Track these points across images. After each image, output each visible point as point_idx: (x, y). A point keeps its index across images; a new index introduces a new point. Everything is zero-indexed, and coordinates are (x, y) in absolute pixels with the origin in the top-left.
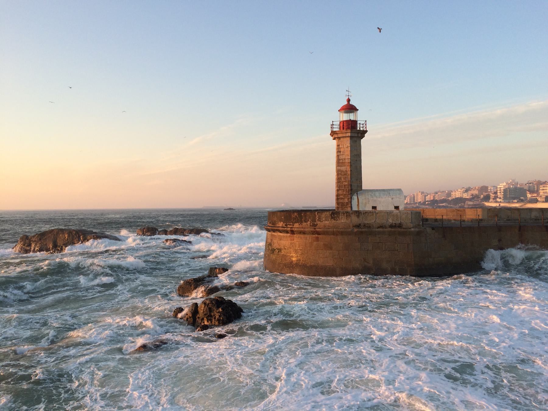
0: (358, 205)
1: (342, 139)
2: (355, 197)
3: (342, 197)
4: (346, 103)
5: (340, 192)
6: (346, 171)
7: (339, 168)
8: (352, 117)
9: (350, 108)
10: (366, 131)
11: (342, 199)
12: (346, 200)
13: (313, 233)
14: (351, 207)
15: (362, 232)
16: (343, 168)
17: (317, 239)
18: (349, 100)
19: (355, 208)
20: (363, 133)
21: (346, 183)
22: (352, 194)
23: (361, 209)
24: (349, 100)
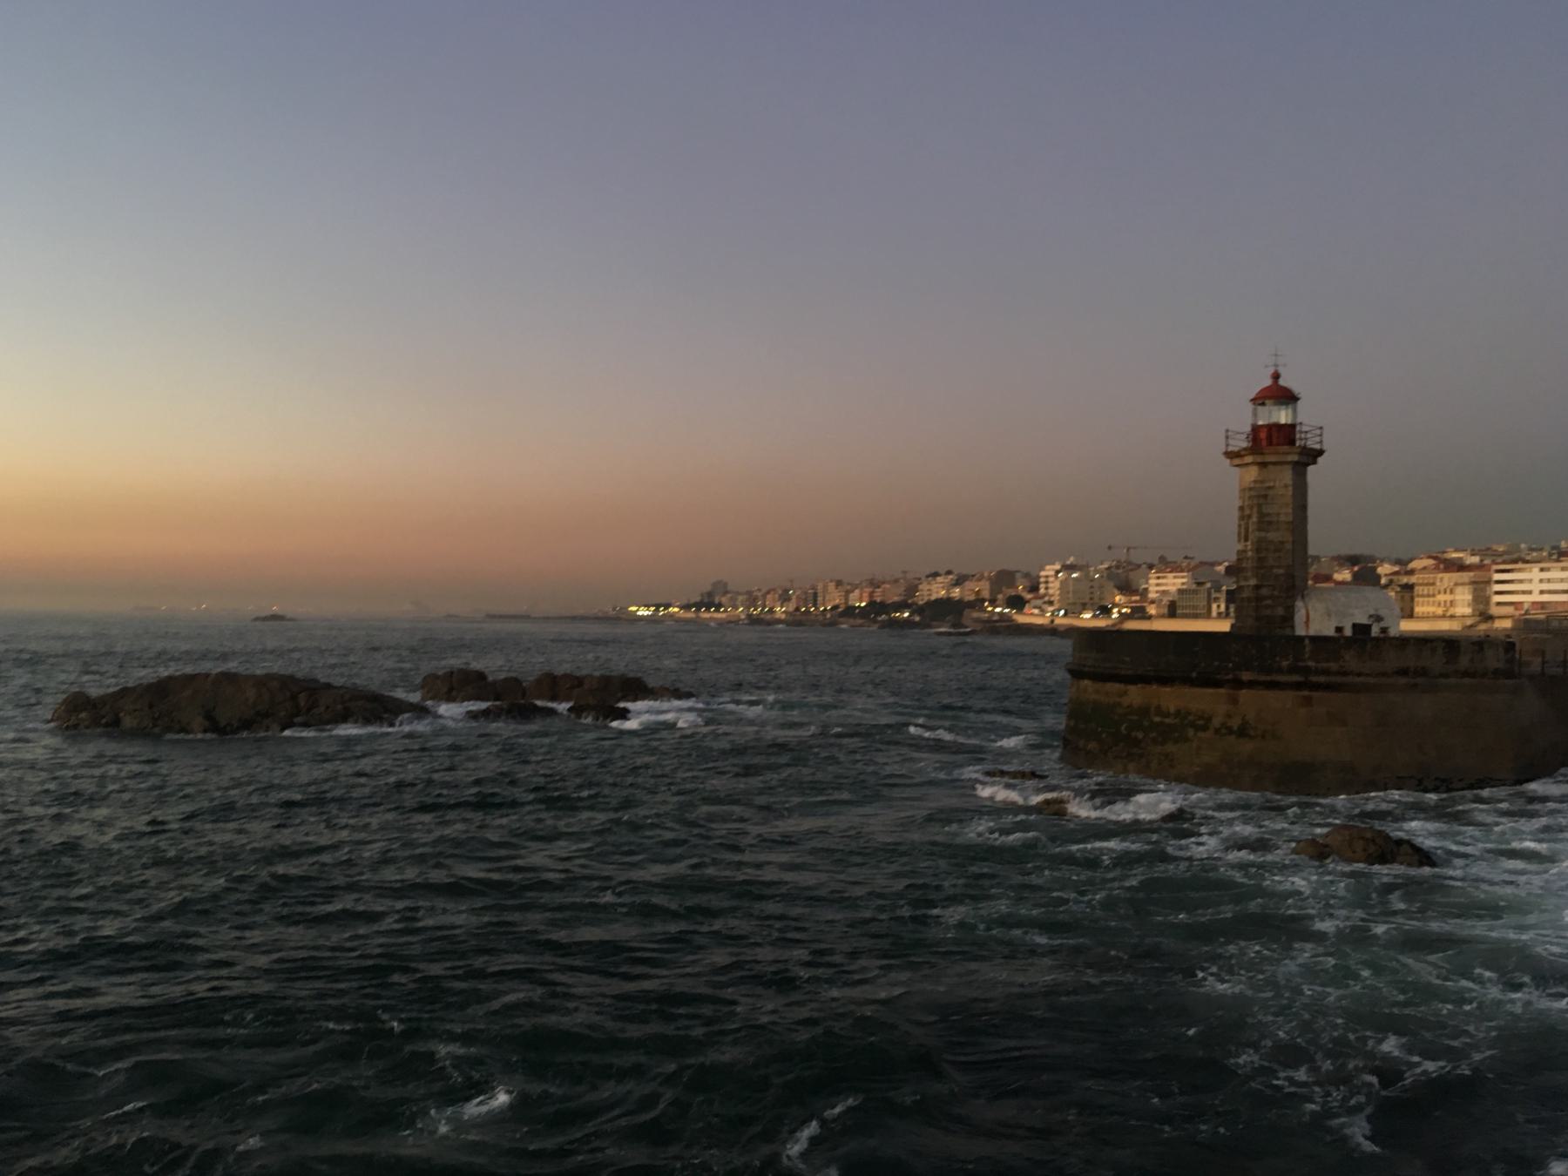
0: (1307, 622)
1: (1271, 467)
2: (1299, 604)
3: (1269, 602)
4: (1268, 382)
5: (1264, 592)
6: (1282, 543)
7: (1263, 534)
8: (1283, 416)
9: (1281, 395)
10: (1321, 452)
11: (1267, 607)
12: (1280, 611)
13: (1298, 686)
14: (1293, 627)
15: (1415, 685)
16: (1272, 536)
17: (1308, 701)
18: (1276, 376)
19: (1300, 631)
20: (1314, 455)
21: (1281, 571)
22: (1293, 598)
23: (1312, 632)
24: (1276, 376)
